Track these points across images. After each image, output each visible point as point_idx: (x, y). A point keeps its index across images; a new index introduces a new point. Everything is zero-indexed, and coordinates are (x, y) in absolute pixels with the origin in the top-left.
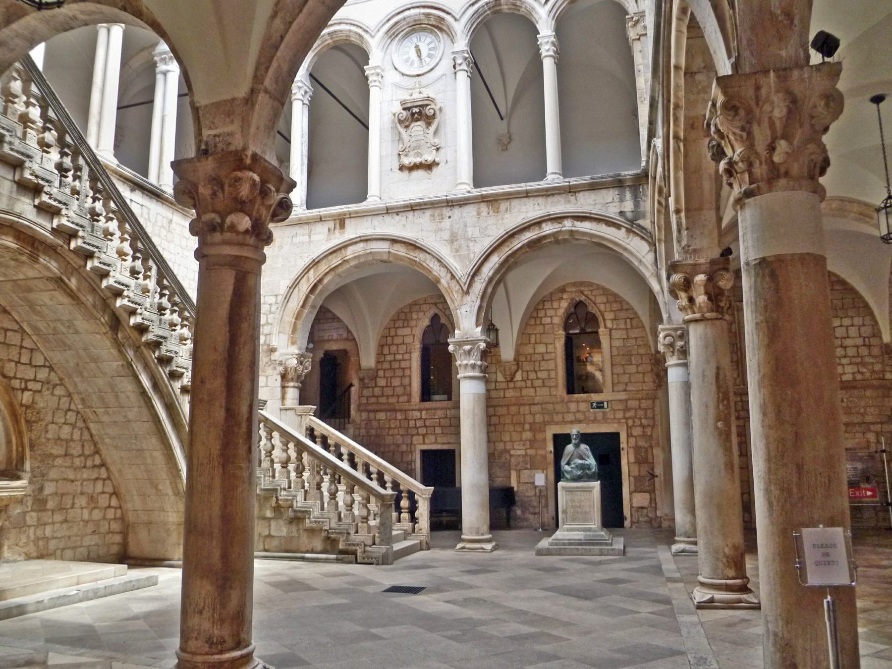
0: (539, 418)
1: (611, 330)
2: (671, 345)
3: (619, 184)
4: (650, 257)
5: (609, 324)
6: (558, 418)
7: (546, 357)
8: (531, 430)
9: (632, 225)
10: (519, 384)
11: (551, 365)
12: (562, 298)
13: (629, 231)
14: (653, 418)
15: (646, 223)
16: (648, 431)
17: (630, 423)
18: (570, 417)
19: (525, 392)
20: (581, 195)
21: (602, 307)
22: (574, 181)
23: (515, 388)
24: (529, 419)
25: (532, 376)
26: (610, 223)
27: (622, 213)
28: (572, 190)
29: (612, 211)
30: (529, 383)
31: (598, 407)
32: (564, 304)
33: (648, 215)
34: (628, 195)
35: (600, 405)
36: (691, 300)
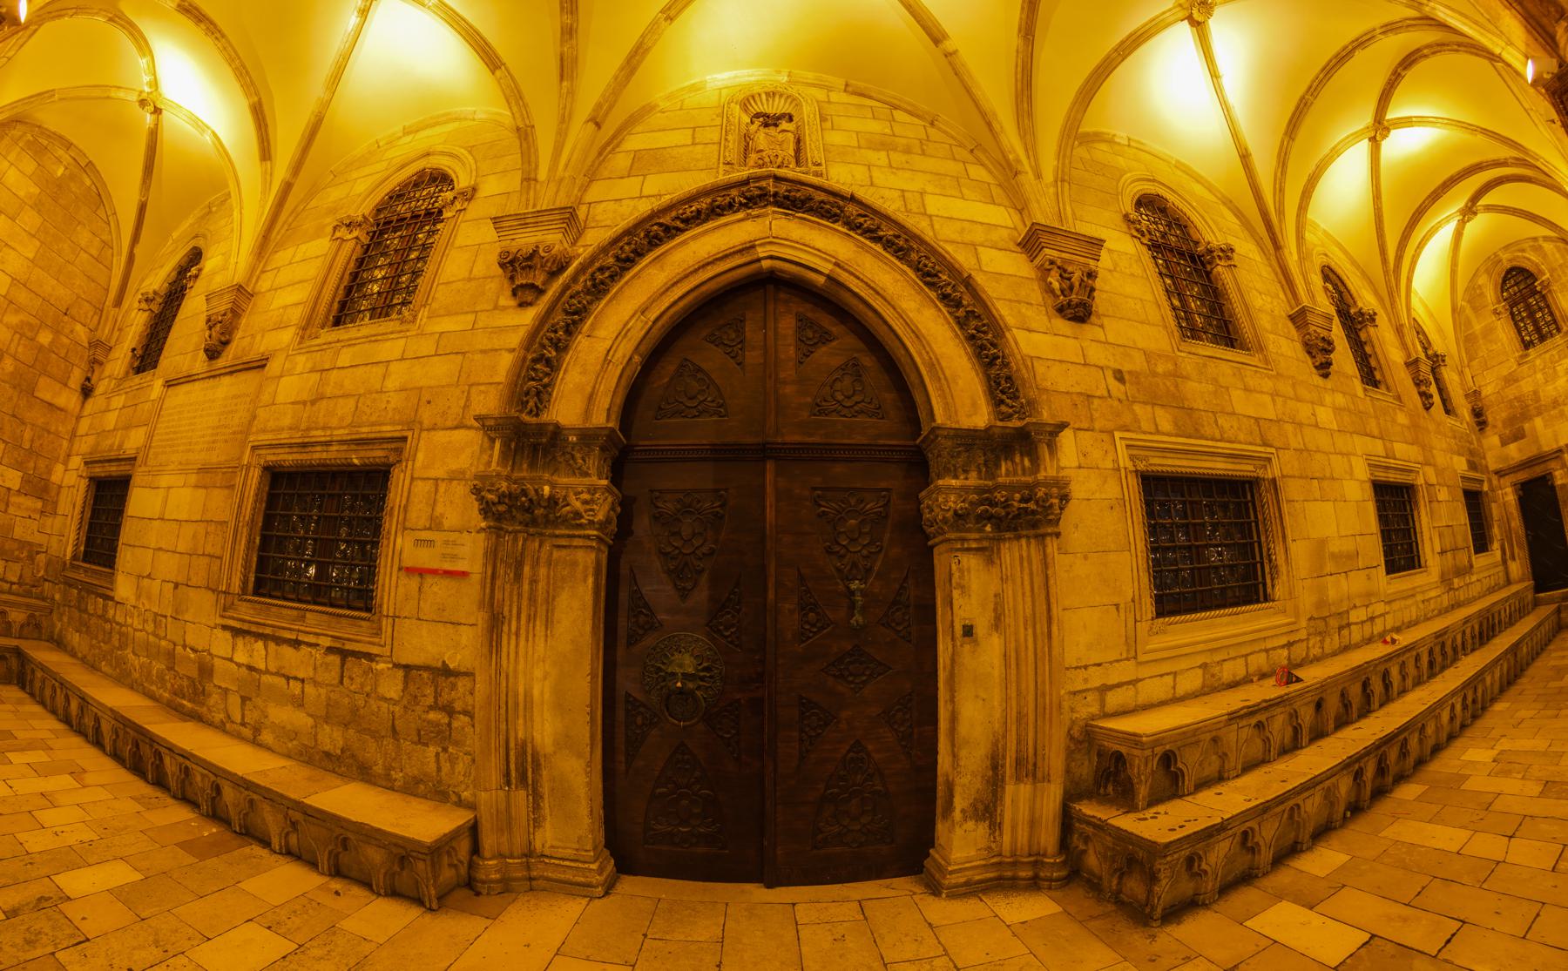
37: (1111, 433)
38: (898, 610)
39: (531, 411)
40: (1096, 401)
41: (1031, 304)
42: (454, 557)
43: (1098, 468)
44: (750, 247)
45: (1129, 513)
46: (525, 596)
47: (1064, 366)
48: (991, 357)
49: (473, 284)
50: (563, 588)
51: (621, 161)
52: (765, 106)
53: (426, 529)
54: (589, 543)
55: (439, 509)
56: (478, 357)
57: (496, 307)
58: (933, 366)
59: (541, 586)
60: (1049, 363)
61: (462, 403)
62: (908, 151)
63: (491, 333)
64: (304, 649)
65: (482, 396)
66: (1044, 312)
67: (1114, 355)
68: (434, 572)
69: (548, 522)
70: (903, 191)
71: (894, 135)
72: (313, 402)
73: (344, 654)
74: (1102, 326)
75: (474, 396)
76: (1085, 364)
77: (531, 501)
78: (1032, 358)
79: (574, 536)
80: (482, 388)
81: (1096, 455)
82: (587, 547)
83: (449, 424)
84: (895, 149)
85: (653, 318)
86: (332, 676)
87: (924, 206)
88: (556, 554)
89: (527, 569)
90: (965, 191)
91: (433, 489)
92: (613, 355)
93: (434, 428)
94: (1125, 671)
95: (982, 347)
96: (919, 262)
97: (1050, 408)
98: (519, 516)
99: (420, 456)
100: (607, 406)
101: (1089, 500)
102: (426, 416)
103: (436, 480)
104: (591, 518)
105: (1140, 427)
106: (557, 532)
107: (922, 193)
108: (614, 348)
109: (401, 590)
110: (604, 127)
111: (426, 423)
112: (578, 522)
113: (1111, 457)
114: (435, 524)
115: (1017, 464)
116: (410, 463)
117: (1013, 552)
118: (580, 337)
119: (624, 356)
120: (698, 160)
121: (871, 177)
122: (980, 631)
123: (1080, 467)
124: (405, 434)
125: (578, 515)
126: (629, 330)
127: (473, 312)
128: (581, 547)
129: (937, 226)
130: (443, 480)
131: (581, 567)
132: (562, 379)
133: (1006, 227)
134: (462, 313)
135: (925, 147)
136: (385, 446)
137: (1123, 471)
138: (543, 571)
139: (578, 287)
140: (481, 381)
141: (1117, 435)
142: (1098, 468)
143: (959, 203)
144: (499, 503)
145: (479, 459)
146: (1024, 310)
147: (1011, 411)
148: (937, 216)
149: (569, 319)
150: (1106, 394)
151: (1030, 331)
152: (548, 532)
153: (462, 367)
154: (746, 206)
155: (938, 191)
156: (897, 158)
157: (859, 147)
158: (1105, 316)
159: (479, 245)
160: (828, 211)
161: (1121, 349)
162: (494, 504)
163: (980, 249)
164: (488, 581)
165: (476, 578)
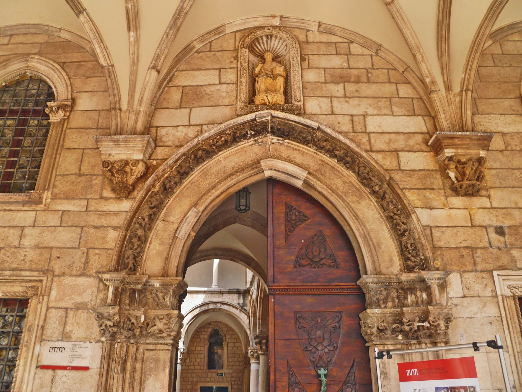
0: (195, 379)
1: (228, 343)
2: (253, 355)
3: (238, 292)
4: (248, 321)
5: (227, 340)
6: (203, 379)
7: (200, 352)
8: (191, 384)
9: (242, 308)
10: (187, 364)
11: (202, 356)
12: (209, 327)
13: (241, 311)
14: (242, 381)
15: (247, 308)
16: (240, 386)
17: (233, 383)
18: (208, 379)
19: (190, 367)
20: (224, 295)
21: (225, 333)
22: (222, 290)
23: (186, 365)
24: (191, 379)
25: (194, 360)
26: (234, 307)
27: (238, 304)
28: (221, 293)
29: (235, 303)
30: (192, 364)
31: (220, 376)
32: (210, 330)
33: (248, 305)
34: (241, 297)
35: (221, 375)
36: (261, 348)
37: (491, 272)
38: (348, 387)
39: (131, 268)
40: (479, 252)
41: (433, 189)
42: (81, 357)
43: (479, 296)
45: (506, 326)
46: (127, 381)
47: (455, 230)
48: (402, 231)
49: (83, 178)
50: (150, 375)
51: (175, 96)
52: (266, 46)
53: (58, 340)
54: (166, 347)
55: (68, 328)
56: (92, 230)
57: (102, 198)
59: (138, 374)
60: (444, 229)
61: (83, 260)
62: (358, 81)
63: (100, 214)
65: (97, 257)
66: (443, 194)
67: (497, 216)
68: (64, 368)
69: (141, 335)
70: (352, 116)
71: (349, 68)
74: (489, 197)
75: (91, 256)
76: (472, 226)
77: (133, 323)
78: (431, 227)
79: (158, 344)
80: (97, 251)
81: (477, 288)
82: (166, 350)
83: (74, 272)
84: (349, 81)
85: (201, 209)
87: (365, 126)
88: (147, 354)
89: (129, 365)
90: (395, 109)
91: (64, 315)
92: (179, 233)
93: (64, 274)
95: (397, 225)
96: (359, 171)
97: (443, 259)
98: (126, 333)
99: (54, 293)
100: (176, 265)
101: (471, 318)
102: (57, 267)
103: (67, 309)
104: (169, 333)
105: (516, 266)
106: (148, 342)
107: (365, 116)
108: (179, 229)
109: (37, 381)
110: (161, 72)
111: (56, 273)
112: (161, 335)
113: (489, 288)
115: (418, 297)
116: (46, 298)
118: (158, 221)
119: (186, 234)
120: (224, 98)
121: (332, 107)
123: (464, 297)
124: (41, 278)
125: (161, 331)
126: (188, 218)
127: (86, 199)
128: (162, 350)
129: (373, 141)
130: (71, 309)
131: (162, 362)
132: (149, 247)
133: (421, 133)
134: (77, 199)
135: (370, 75)
136: (24, 284)
137: (500, 298)
138: (139, 365)
139: (156, 189)
140: (95, 247)
141: (495, 273)
142: (479, 296)
143: (390, 119)
144: (114, 326)
145: (97, 297)
146: (427, 195)
147: (413, 264)
148: (374, 133)
149: (152, 211)
150: (487, 245)
151: (431, 208)
152: (142, 341)
153: (81, 237)
154: (255, 135)
155: (375, 112)
156: (351, 87)
157: (326, 82)
158: (492, 188)
159: (84, 149)
160: (304, 138)
161: (504, 211)
162: (110, 326)
163: (401, 154)
164: (105, 373)
165: (94, 372)
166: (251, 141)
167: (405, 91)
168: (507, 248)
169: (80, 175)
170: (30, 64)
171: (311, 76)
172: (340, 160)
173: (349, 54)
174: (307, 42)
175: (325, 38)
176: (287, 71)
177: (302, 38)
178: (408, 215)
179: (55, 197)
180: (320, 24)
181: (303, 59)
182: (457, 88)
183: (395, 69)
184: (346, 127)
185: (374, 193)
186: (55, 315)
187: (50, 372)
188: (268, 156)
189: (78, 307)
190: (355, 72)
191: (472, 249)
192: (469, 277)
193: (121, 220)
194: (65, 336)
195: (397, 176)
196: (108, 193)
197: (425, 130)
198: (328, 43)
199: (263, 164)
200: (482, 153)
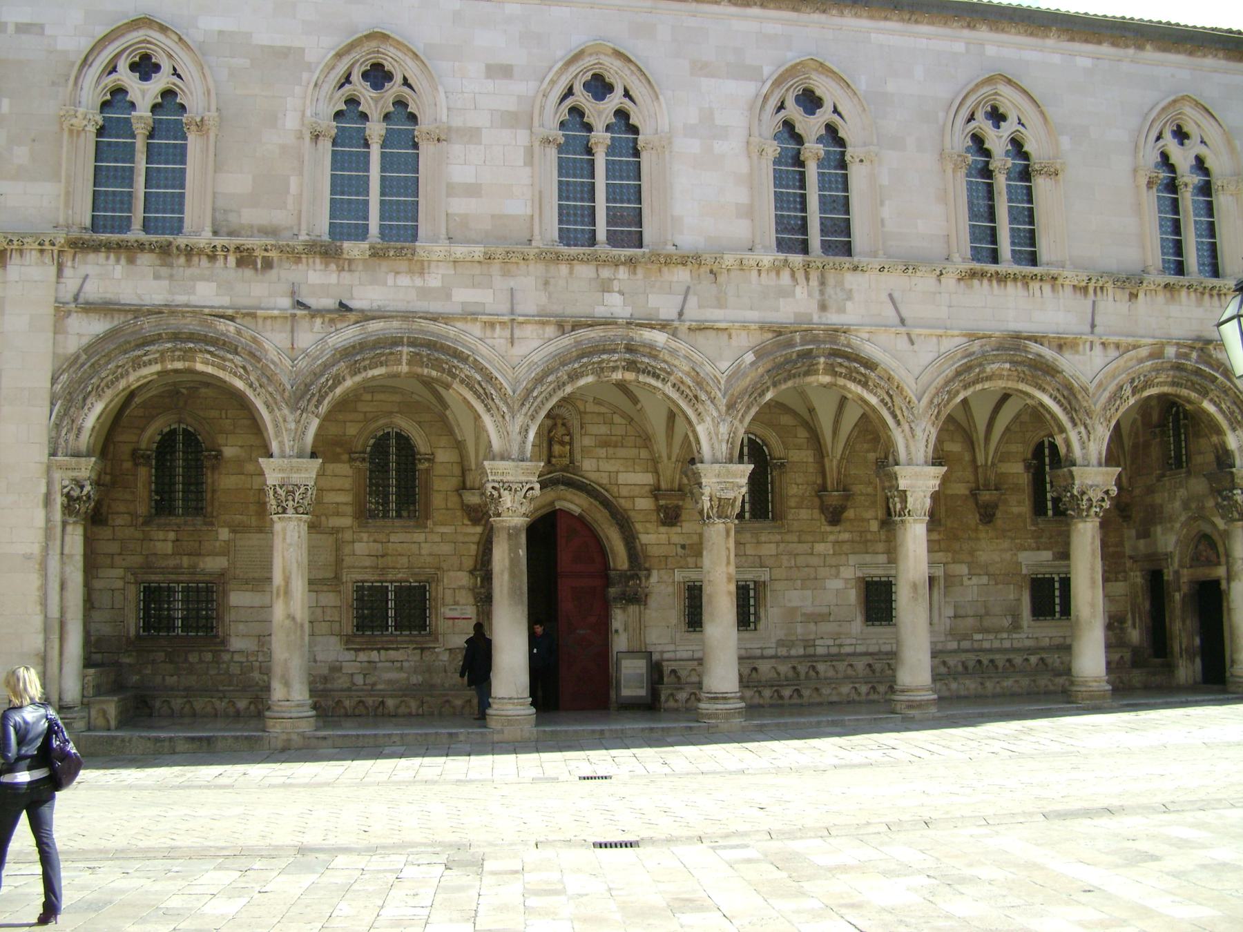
37: (674, 569)
44: (552, 503)
58: (612, 550)
62: (615, 446)
64: (401, 651)
72: (382, 556)
73: (422, 649)
81: (665, 578)
86: (417, 658)
90: (636, 467)
94: (672, 647)
102: (445, 566)
114: (456, 603)
117: (633, 609)
122: (621, 631)
156: (611, 450)
166: (549, 489)
167: (644, 454)
168: (685, 556)
169: (447, 509)
170: (394, 420)
171: (587, 441)
172: (601, 503)
173: (612, 423)
174: (585, 413)
175: (597, 409)
176: (572, 439)
177: (582, 408)
178: (634, 539)
179: (435, 524)
180: (595, 398)
181: (582, 428)
182: (673, 459)
183: (640, 436)
184: (605, 481)
185: (617, 523)
186: (448, 592)
187: (451, 621)
188: (559, 499)
189: (460, 588)
190: (614, 438)
191: (666, 557)
192: (662, 572)
193: (476, 539)
194: (456, 603)
195: (632, 514)
196: (466, 522)
197: (652, 482)
198: (599, 414)
199: (556, 504)
200: (681, 503)
